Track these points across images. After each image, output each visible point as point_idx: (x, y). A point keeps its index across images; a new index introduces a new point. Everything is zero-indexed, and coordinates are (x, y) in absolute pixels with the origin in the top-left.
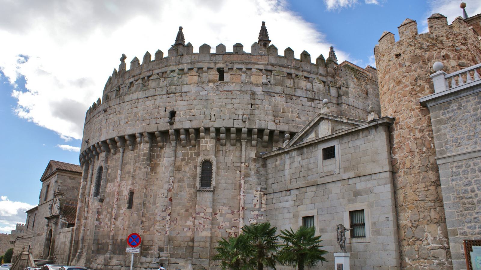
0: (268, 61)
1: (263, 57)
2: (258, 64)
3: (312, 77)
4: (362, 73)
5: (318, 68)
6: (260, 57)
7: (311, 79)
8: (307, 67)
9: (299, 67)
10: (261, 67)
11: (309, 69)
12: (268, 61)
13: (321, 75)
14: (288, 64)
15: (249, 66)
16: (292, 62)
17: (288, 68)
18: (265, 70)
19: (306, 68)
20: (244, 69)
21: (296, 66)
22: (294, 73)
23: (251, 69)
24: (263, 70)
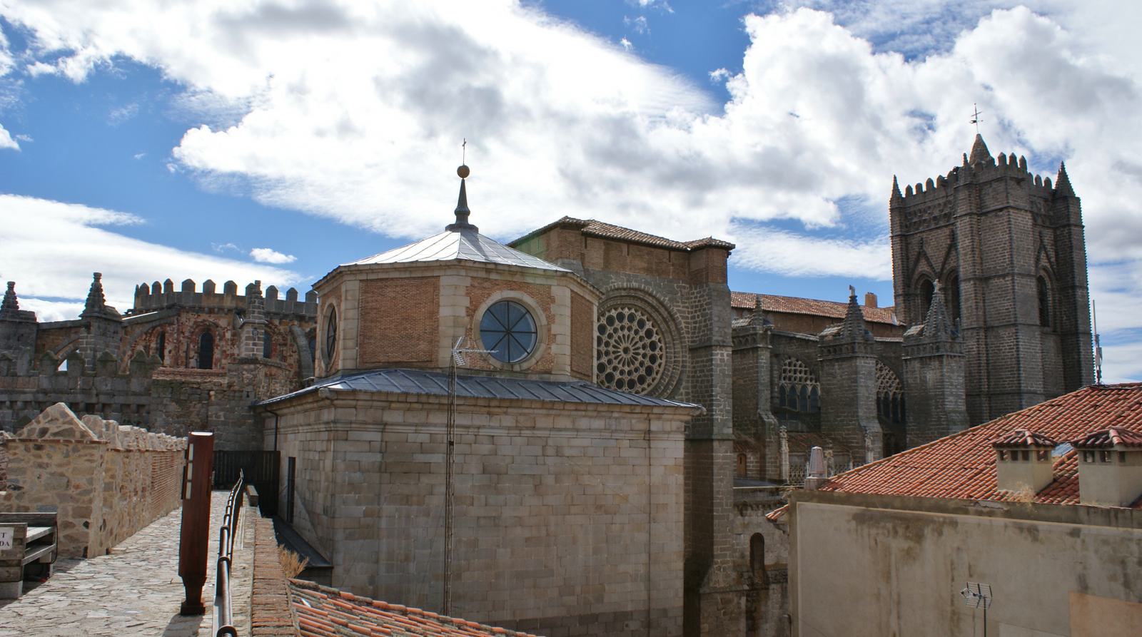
0: (38, 386)
1: (32, 378)
2: (25, 393)
3: (116, 402)
4: (195, 386)
5: (128, 382)
6: (27, 379)
7: (114, 405)
8: (106, 385)
9: (90, 389)
10: (29, 397)
11: (109, 387)
12: (38, 386)
13: (135, 394)
14: (70, 387)
15: (14, 397)
16: (77, 382)
17: (71, 394)
18: (36, 402)
19: (104, 388)
20: (8, 403)
21: (85, 387)
22: (82, 402)
23: (16, 402)
24: (33, 403)
